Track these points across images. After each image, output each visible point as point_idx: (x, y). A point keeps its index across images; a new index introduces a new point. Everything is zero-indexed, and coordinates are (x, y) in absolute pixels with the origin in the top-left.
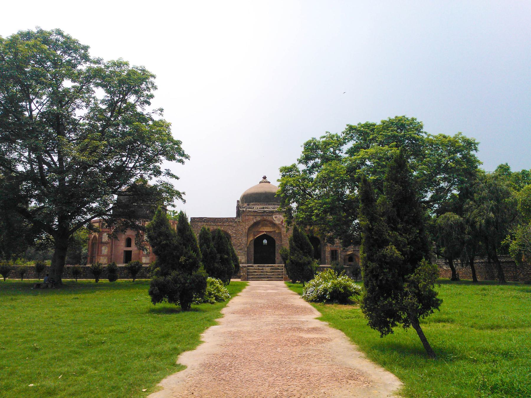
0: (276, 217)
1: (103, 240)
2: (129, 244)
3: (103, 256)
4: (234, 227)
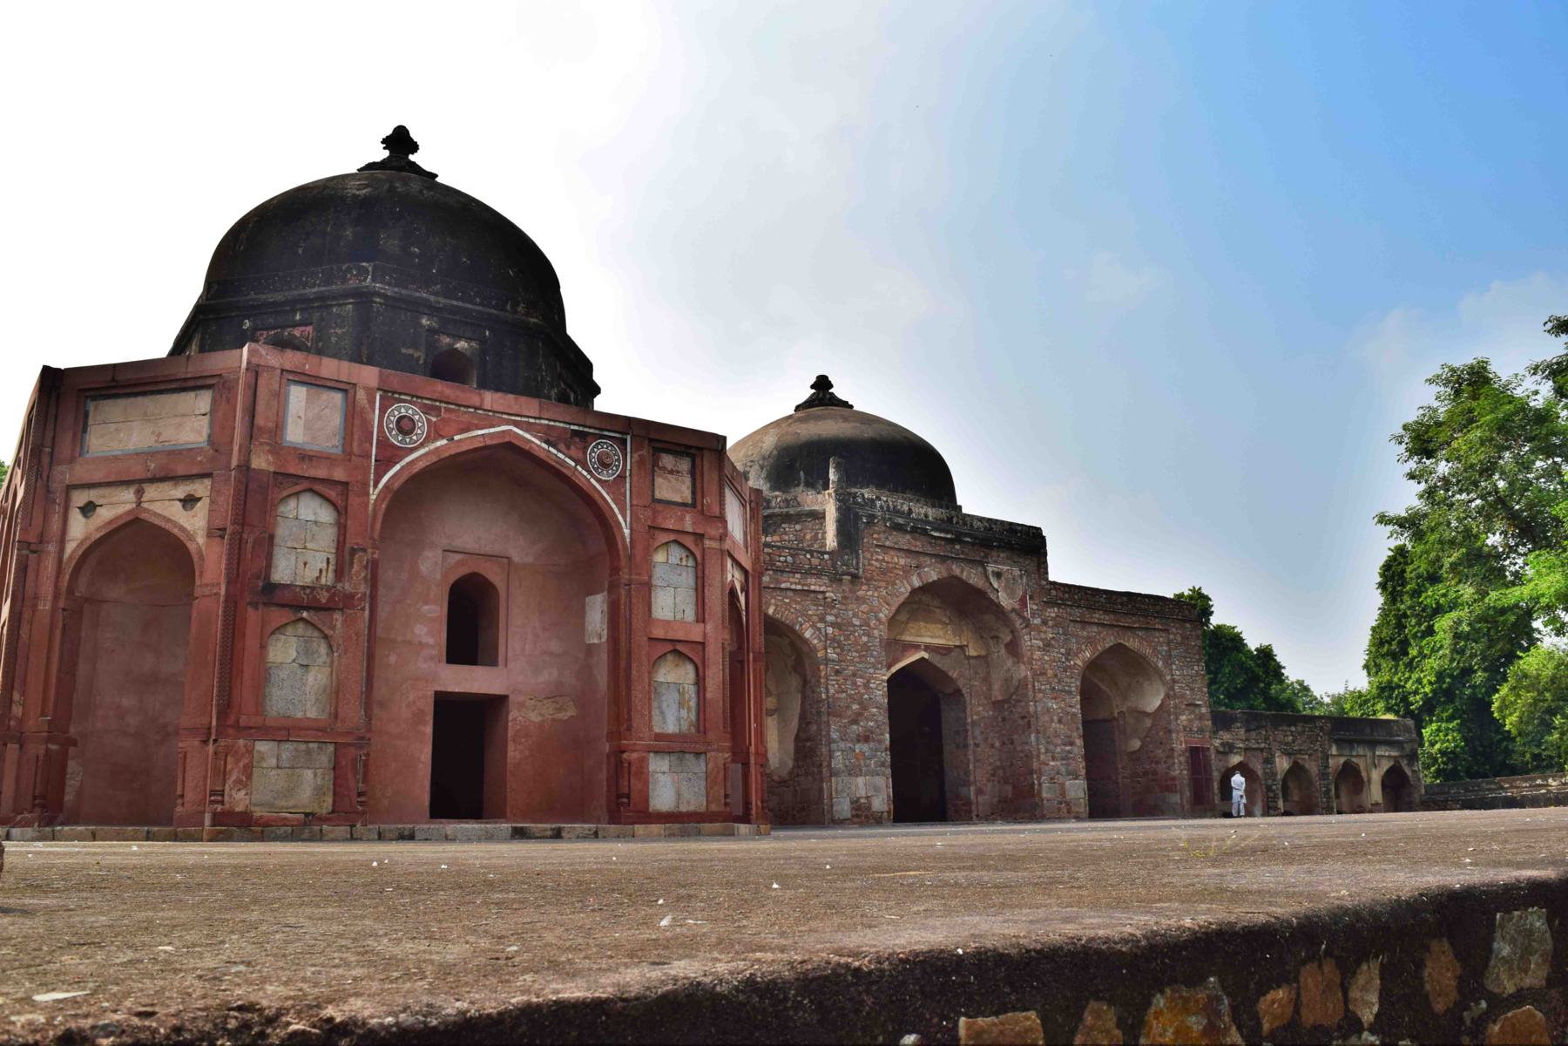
0: (998, 575)
1: (283, 571)
2: (471, 623)
3: (285, 731)
4: (829, 605)
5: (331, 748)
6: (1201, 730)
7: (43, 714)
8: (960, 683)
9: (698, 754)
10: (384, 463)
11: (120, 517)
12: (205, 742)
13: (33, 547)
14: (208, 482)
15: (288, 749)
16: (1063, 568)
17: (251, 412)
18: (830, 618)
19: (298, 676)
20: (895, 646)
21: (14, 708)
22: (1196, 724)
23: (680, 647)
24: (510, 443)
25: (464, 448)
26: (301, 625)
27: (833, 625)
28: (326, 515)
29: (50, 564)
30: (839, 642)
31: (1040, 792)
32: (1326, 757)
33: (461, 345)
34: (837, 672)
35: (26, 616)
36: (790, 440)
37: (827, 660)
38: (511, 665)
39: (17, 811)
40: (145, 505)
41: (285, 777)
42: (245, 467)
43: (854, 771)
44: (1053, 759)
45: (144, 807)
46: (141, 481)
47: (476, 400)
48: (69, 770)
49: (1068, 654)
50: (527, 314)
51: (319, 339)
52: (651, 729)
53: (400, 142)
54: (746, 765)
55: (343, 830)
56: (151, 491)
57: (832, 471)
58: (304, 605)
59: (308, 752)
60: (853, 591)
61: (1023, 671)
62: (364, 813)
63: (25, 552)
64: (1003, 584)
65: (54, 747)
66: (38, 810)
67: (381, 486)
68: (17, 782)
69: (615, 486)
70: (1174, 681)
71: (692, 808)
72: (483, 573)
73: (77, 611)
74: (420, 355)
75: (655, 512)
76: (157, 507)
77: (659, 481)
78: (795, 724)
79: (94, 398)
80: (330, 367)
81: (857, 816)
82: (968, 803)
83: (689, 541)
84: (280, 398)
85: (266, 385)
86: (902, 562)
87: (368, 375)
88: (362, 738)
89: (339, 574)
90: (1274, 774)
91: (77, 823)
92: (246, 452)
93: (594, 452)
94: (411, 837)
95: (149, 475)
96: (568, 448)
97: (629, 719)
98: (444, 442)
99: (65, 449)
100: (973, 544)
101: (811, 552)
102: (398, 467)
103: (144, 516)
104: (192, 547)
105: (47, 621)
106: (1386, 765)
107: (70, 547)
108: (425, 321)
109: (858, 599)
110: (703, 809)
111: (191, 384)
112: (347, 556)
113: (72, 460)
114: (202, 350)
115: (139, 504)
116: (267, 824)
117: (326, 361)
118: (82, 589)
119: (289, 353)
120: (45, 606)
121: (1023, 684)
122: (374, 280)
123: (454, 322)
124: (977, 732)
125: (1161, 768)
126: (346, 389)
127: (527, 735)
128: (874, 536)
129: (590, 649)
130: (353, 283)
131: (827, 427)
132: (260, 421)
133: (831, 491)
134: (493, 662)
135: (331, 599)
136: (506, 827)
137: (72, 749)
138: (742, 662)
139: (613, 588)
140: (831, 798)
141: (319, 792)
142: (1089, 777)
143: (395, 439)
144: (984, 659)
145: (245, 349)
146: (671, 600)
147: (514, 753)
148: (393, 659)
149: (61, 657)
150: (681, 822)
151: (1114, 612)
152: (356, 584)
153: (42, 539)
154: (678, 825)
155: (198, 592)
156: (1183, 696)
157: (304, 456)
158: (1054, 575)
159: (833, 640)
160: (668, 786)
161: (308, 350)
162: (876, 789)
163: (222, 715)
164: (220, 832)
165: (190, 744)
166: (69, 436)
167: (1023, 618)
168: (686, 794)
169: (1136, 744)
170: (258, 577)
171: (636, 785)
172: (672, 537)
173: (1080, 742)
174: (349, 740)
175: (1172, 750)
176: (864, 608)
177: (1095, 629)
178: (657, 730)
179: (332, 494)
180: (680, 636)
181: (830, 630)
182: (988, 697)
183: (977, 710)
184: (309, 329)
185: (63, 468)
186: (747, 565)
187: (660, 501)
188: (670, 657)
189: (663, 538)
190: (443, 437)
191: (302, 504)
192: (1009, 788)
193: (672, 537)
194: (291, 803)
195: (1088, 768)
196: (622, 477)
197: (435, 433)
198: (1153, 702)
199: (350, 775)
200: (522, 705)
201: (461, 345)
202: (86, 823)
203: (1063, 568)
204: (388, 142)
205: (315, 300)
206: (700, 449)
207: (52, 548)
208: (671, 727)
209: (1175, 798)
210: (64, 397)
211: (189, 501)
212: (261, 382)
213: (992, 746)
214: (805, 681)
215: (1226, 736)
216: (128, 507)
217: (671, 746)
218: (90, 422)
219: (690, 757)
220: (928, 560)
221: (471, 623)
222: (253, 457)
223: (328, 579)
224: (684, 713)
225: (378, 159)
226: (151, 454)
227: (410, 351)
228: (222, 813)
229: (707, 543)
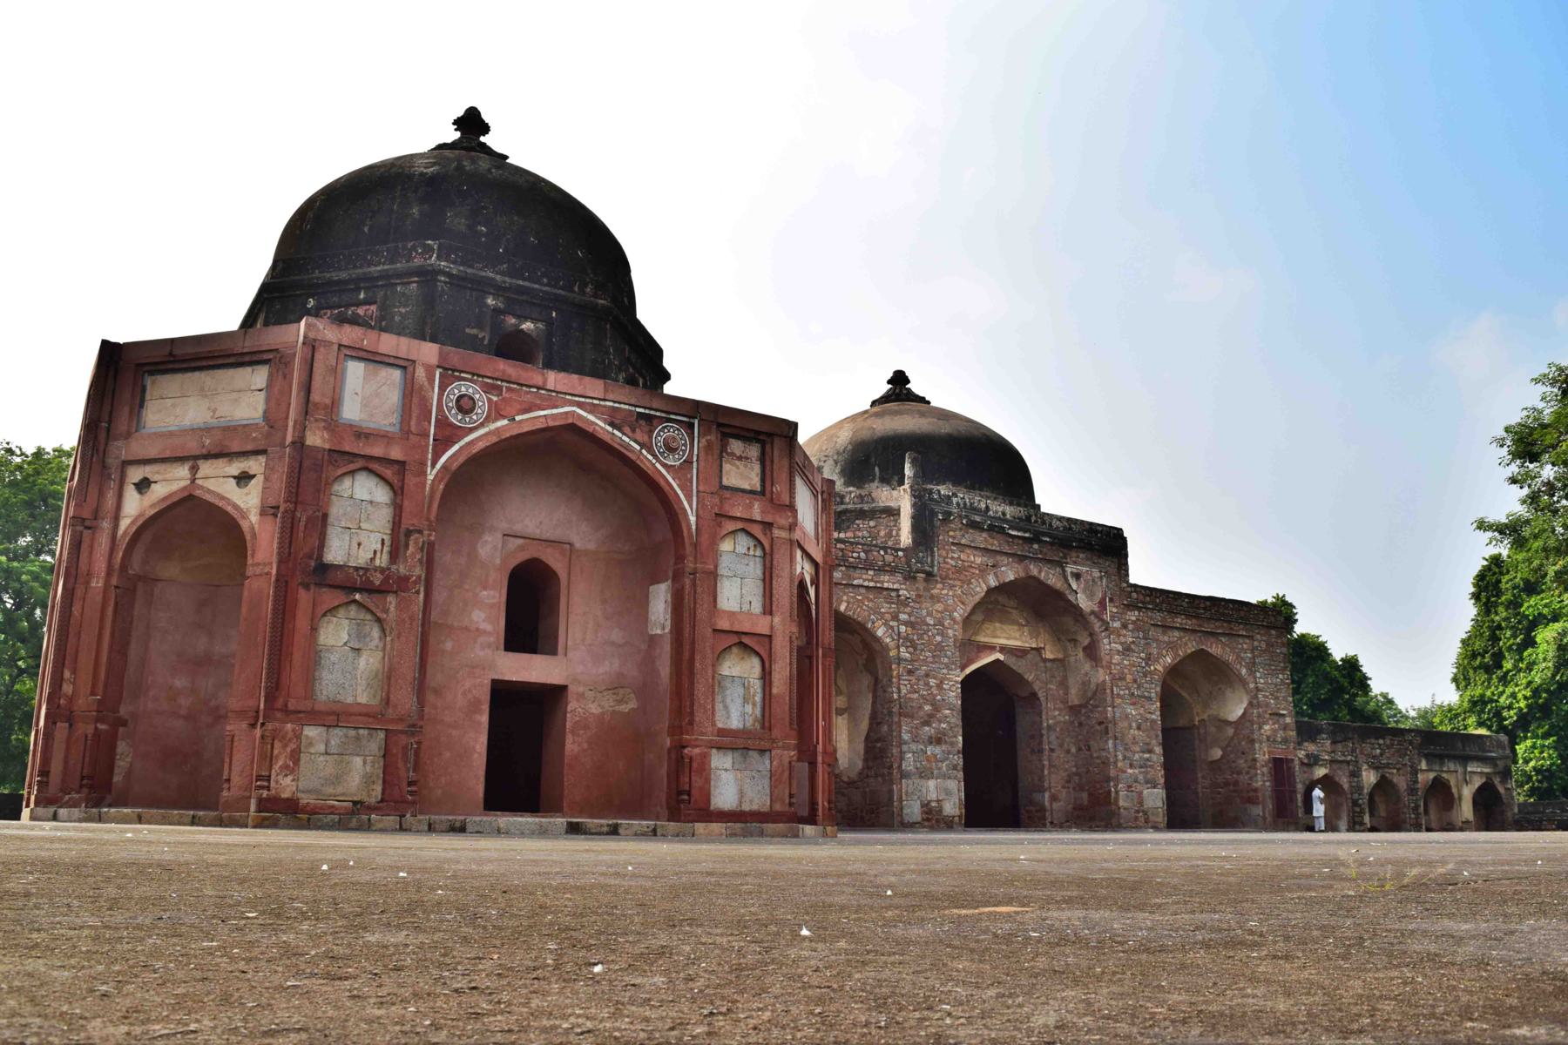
0: (1077, 576)
1: (337, 550)
2: (530, 610)
3: (335, 716)
4: (904, 603)
5: (382, 735)
6: (1285, 741)
7: (93, 693)
8: (1036, 687)
9: (762, 751)
10: (443, 443)
11: (170, 495)
12: (253, 726)
13: (87, 523)
14: (262, 459)
15: (337, 735)
16: (1144, 570)
17: (307, 388)
18: (903, 617)
19: (349, 657)
20: (970, 647)
21: (65, 686)
22: (1280, 734)
23: (746, 640)
24: (573, 425)
25: (526, 429)
26: (353, 607)
27: (906, 623)
28: (382, 495)
29: (103, 541)
30: (912, 641)
31: (1117, 799)
32: (1415, 772)
33: (527, 326)
34: (910, 672)
35: (79, 592)
36: (865, 435)
37: (899, 660)
38: (570, 654)
39: (65, 791)
40: (199, 482)
41: (335, 764)
42: (299, 444)
43: (925, 774)
44: (1131, 766)
45: (192, 792)
46: (196, 458)
47: (538, 380)
48: (119, 750)
49: (1148, 659)
50: (596, 296)
51: (381, 318)
52: (714, 724)
53: (472, 123)
54: (813, 764)
55: (392, 820)
56: (206, 468)
57: (907, 466)
58: (357, 587)
59: (358, 738)
60: (928, 590)
61: (1101, 676)
62: (414, 803)
63: (80, 528)
64: (1083, 586)
65: (102, 727)
66: (85, 790)
67: (438, 466)
68: (66, 762)
69: (682, 471)
70: (1258, 689)
71: (755, 807)
72: (544, 558)
73: (130, 588)
74: (485, 335)
75: (722, 500)
76: (211, 485)
77: (727, 467)
78: (864, 725)
79: (151, 373)
80: (388, 343)
81: (928, 820)
82: (1043, 809)
83: (757, 530)
84: (337, 374)
85: (323, 360)
86: (978, 560)
87: (428, 352)
88: (414, 726)
89: (394, 555)
90: (1362, 788)
91: (126, 805)
92: (302, 428)
93: (660, 436)
94: (460, 829)
95: (204, 451)
96: (633, 431)
97: (692, 713)
98: (505, 422)
99: (122, 425)
100: (1051, 544)
101: (885, 549)
102: (456, 447)
103: (198, 493)
104: (244, 525)
105: (99, 598)
106: (1478, 782)
107: (124, 524)
108: (490, 301)
109: (932, 597)
110: (766, 809)
111: (247, 359)
112: (402, 538)
113: (128, 436)
114: (266, 324)
115: (193, 481)
116: (314, 811)
117: (385, 337)
118: (136, 567)
119: (347, 328)
120: (97, 583)
121: (1101, 688)
122: (439, 258)
123: (519, 302)
124: (1053, 738)
125: (1244, 778)
126: (405, 365)
127: (586, 727)
128: (953, 533)
129: (653, 640)
130: (417, 262)
131: (904, 422)
132: (316, 397)
133: (906, 486)
134: (553, 651)
135: (387, 579)
136: (561, 821)
137: (121, 729)
138: (810, 658)
139: (677, 577)
140: (901, 800)
141: (368, 780)
142: (1168, 786)
143: (455, 418)
144: (1061, 662)
145: (303, 323)
146: (737, 591)
147: (572, 745)
148: (449, 645)
149: (112, 635)
150: (744, 822)
151: (1197, 617)
152: (410, 566)
153: (96, 515)
154: (739, 825)
155: (250, 571)
156: (1267, 705)
157: (361, 434)
158: (1134, 578)
159: (906, 639)
160: (731, 783)
161: (372, 328)
162: (948, 792)
163: (271, 697)
164: (265, 819)
165: (237, 727)
166: (126, 409)
167: (1102, 620)
168: (750, 793)
169: (1217, 753)
170: (310, 557)
171: (697, 782)
172: (740, 525)
173: (1158, 750)
174: (400, 728)
175: (1255, 760)
176: (939, 607)
177: (1177, 634)
178: (720, 725)
179: (388, 473)
180: (746, 627)
181: (903, 629)
182: (1064, 702)
183: (1053, 715)
184: (373, 308)
185: (119, 443)
186: (818, 557)
187: (727, 488)
188: (735, 650)
189: (731, 526)
190: (504, 417)
191: (357, 483)
192: (1085, 795)
193: (740, 525)
194: (340, 790)
195: (1166, 777)
196: (689, 462)
197: (496, 412)
198: (1235, 709)
199: (400, 764)
200: (581, 696)
201: (527, 326)
202: (134, 806)
203: (1144, 570)
204: (459, 123)
205: (380, 278)
206: (770, 435)
207: (106, 525)
208: (735, 723)
209: (1257, 811)
210: (122, 373)
211: (243, 479)
212: (317, 356)
213: (1068, 752)
214: (877, 681)
215: (1312, 748)
216: (183, 484)
217: (734, 742)
218: (148, 397)
219: (754, 754)
220: (1005, 560)
221: (530, 610)
222: (308, 433)
223: (382, 561)
224: (749, 709)
225: (449, 141)
226: (208, 430)
227: (474, 331)
228: (268, 799)
229: (777, 533)
